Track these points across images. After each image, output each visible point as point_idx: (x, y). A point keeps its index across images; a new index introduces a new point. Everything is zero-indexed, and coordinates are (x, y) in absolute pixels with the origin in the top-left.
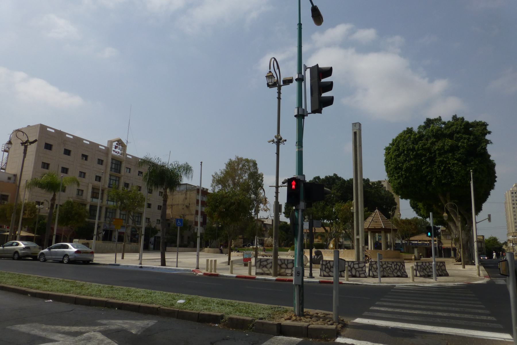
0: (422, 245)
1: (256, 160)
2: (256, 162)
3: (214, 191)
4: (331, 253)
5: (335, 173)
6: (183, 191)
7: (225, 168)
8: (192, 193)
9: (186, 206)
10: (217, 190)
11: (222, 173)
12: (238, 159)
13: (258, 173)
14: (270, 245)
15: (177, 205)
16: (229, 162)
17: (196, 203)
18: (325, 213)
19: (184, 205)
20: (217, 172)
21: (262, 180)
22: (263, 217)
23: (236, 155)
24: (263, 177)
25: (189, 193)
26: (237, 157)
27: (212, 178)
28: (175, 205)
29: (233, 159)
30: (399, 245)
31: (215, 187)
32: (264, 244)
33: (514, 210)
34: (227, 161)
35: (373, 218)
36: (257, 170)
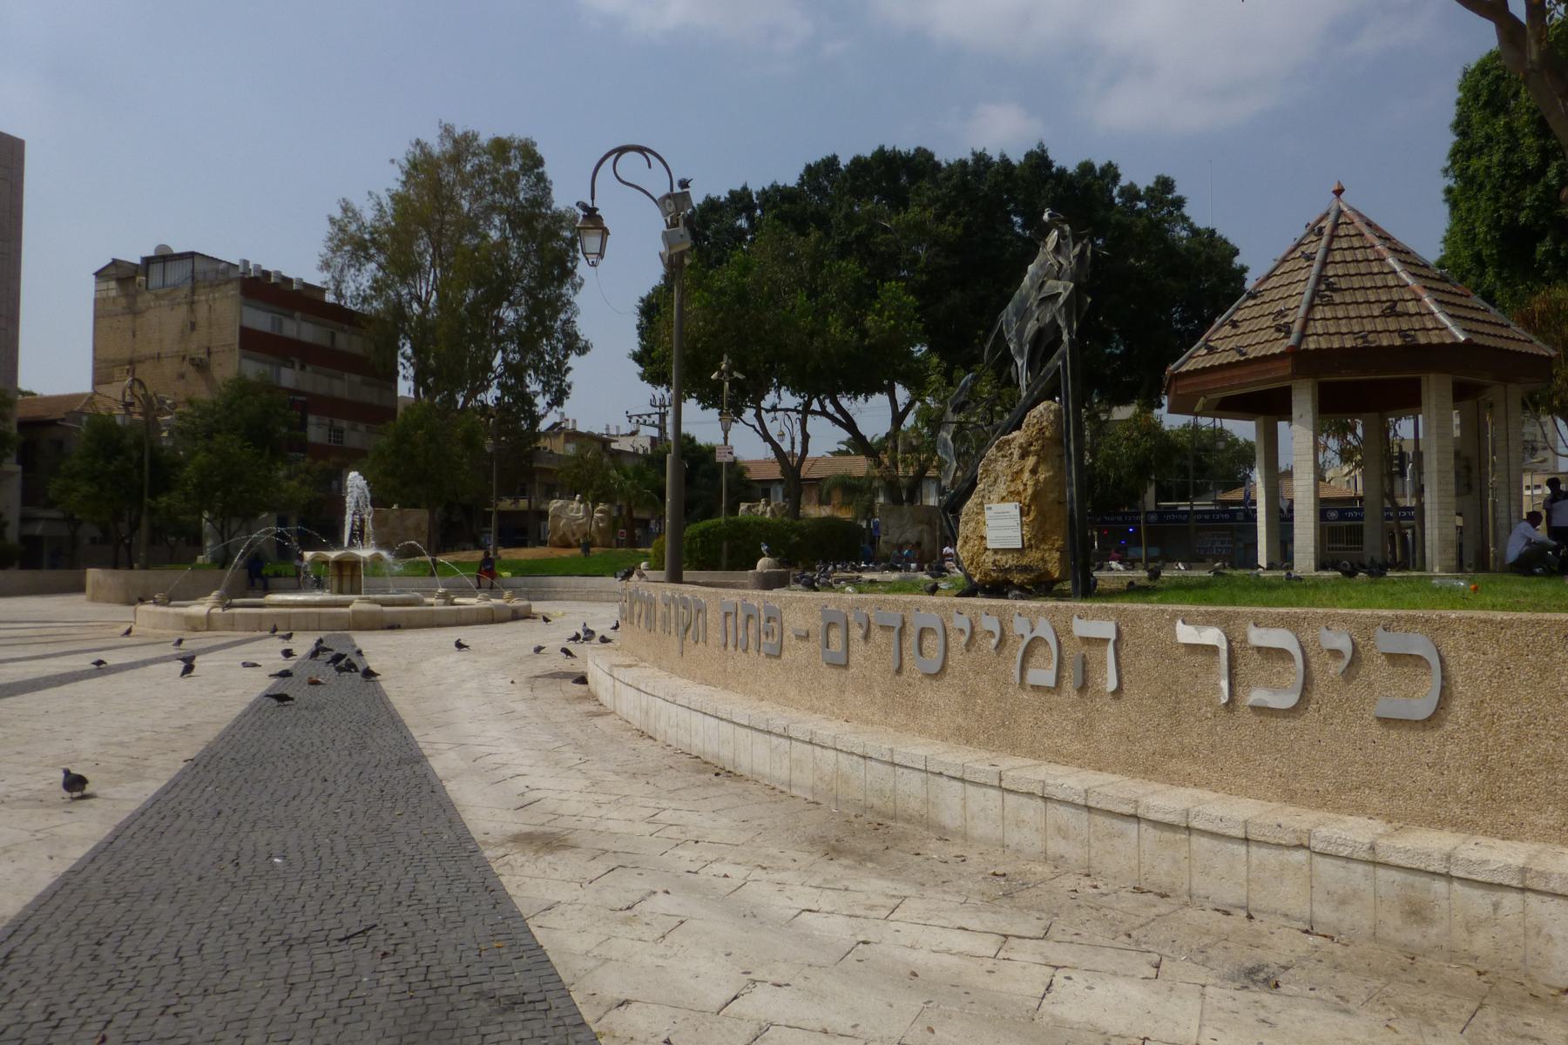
1: (534, 140)
2: (540, 150)
3: (339, 294)
4: (1043, 675)
5: (923, 145)
6: (176, 287)
7: (397, 187)
8: (217, 295)
9: (192, 359)
10: (351, 284)
12: (455, 141)
13: (554, 207)
15: (153, 358)
16: (415, 157)
17: (237, 347)
18: (870, 321)
19: (184, 358)
20: (348, 198)
22: (618, 428)
25: (203, 298)
26: (446, 130)
27: (326, 229)
28: (146, 359)
29: (436, 146)
31: (342, 270)
34: (402, 151)
35: (1324, 264)
36: (547, 191)
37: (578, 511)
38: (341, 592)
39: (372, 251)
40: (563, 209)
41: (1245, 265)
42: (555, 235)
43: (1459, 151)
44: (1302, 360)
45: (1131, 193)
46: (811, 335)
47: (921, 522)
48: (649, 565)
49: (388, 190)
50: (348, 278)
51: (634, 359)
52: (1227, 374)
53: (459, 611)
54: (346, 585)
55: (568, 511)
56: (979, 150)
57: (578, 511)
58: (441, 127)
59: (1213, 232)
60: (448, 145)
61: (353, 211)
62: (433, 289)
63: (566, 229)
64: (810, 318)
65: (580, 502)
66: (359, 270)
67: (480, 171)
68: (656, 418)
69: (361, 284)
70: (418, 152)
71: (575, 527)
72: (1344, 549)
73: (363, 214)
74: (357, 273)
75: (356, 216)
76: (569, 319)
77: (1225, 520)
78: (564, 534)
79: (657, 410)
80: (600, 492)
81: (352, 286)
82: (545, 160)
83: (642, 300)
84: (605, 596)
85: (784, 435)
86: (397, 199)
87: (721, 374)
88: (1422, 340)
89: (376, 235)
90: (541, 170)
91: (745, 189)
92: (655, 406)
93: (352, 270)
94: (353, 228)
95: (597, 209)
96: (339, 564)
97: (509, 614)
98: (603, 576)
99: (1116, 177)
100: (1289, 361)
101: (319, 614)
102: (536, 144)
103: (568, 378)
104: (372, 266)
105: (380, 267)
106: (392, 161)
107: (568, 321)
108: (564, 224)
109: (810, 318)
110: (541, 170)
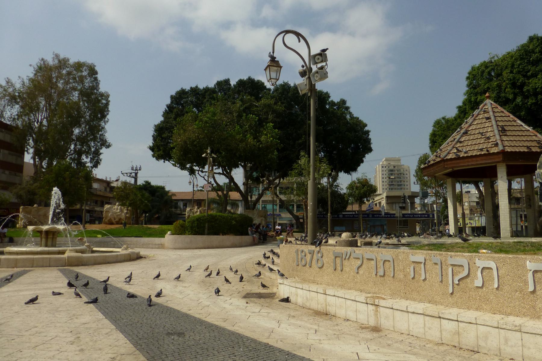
0: (414, 217)
1: (95, 64)
2: (96, 68)
7: (32, 76)
10: (8, 112)
11: (23, 84)
12: (59, 61)
13: (100, 90)
14: (117, 220)
18: (263, 138)
20: (10, 78)
21: (107, 104)
22: (110, 178)
23: (54, 52)
24: (109, 99)
29: (51, 61)
30: (378, 217)
31: (4, 107)
32: (103, 218)
33: (383, 183)
34: (36, 62)
36: (98, 84)
37: (117, 209)
38: (46, 246)
39: (18, 100)
40: (103, 92)
41: (369, 130)
42: (99, 101)
43: (472, 93)
44: (506, 155)
45: (333, 104)
46: (242, 141)
47: (262, 217)
48: (171, 233)
49: (28, 76)
50: (7, 110)
51: (149, 149)
52: (470, 160)
53: (117, 255)
54: (50, 243)
55: (112, 209)
56: (286, 81)
57: (117, 209)
58: (53, 54)
59: (358, 118)
60: (56, 61)
61: (11, 83)
62: (44, 118)
63: (104, 100)
64: (242, 135)
65: (118, 206)
66: (12, 107)
67: (69, 73)
68: (134, 174)
69: (13, 113)
70: (42, 63)
71: (115, 216)
72: (402, 228)
73: (16, 85)
74: (11, 108)
75: (12, 85)
76: (103, 134)
77: (351, 217)
78: (110, 219)
79: (134, 171)
80: (132, 202)
81: (9, 114)
82: (98, 73)
83: (155, 126)
84: (151, 246)
85: (191, 182)
86: (31, 80)
87: (207, 155)
88: (534, 150)
89: (21, 94)
90: (96, 76)
91: (197, 87)
92: (133, 170)
93: (9, 107)
94: (11, 90)
95: (275, 58)
96: (47, 232)
97: (136, 257)
98: (142, 237)
99: (329, 97)
100: (501, 155)
101: (50, 258)
102: (95, 66)
103: (101, 157)
104: (17, 106)
105: (22, 107)
106: (31, 65)
107: (102, 135)
108: (104, 97)
109: (242, 135)
110: (96, 76)
